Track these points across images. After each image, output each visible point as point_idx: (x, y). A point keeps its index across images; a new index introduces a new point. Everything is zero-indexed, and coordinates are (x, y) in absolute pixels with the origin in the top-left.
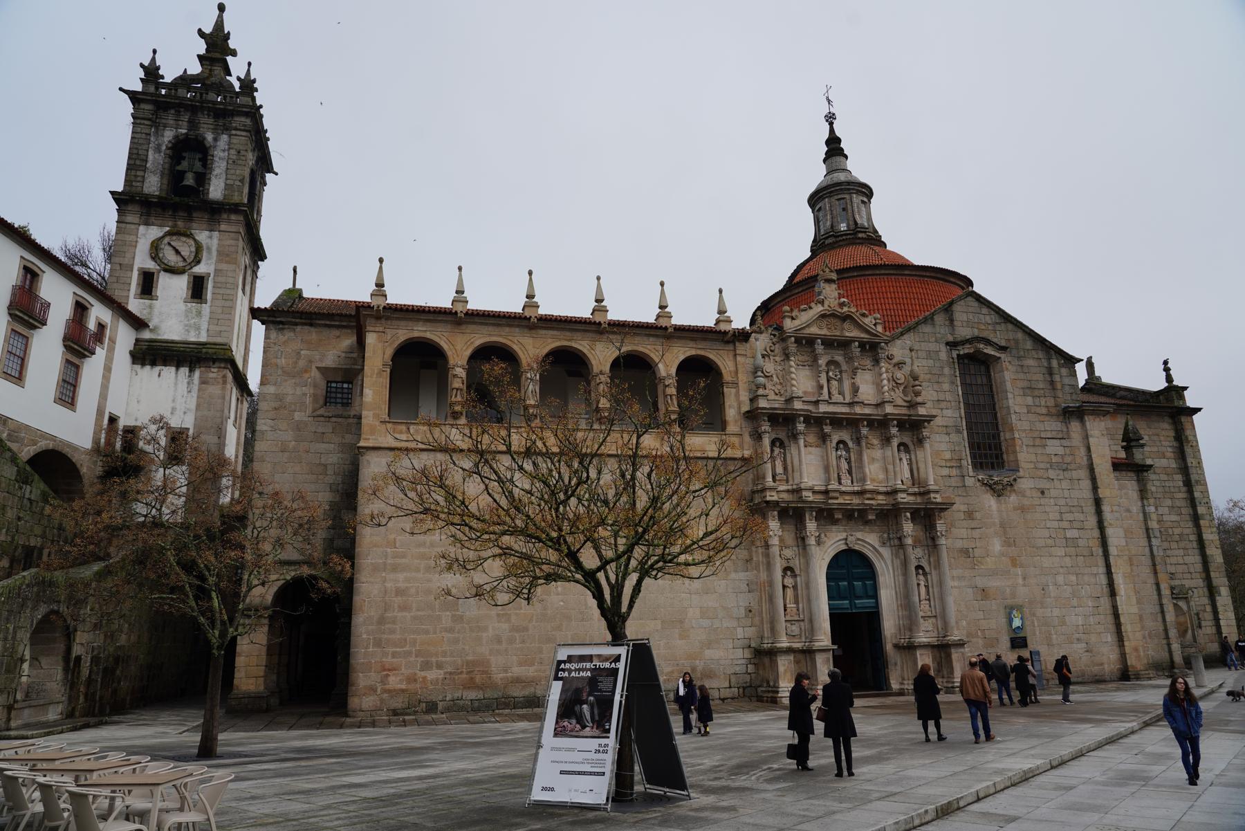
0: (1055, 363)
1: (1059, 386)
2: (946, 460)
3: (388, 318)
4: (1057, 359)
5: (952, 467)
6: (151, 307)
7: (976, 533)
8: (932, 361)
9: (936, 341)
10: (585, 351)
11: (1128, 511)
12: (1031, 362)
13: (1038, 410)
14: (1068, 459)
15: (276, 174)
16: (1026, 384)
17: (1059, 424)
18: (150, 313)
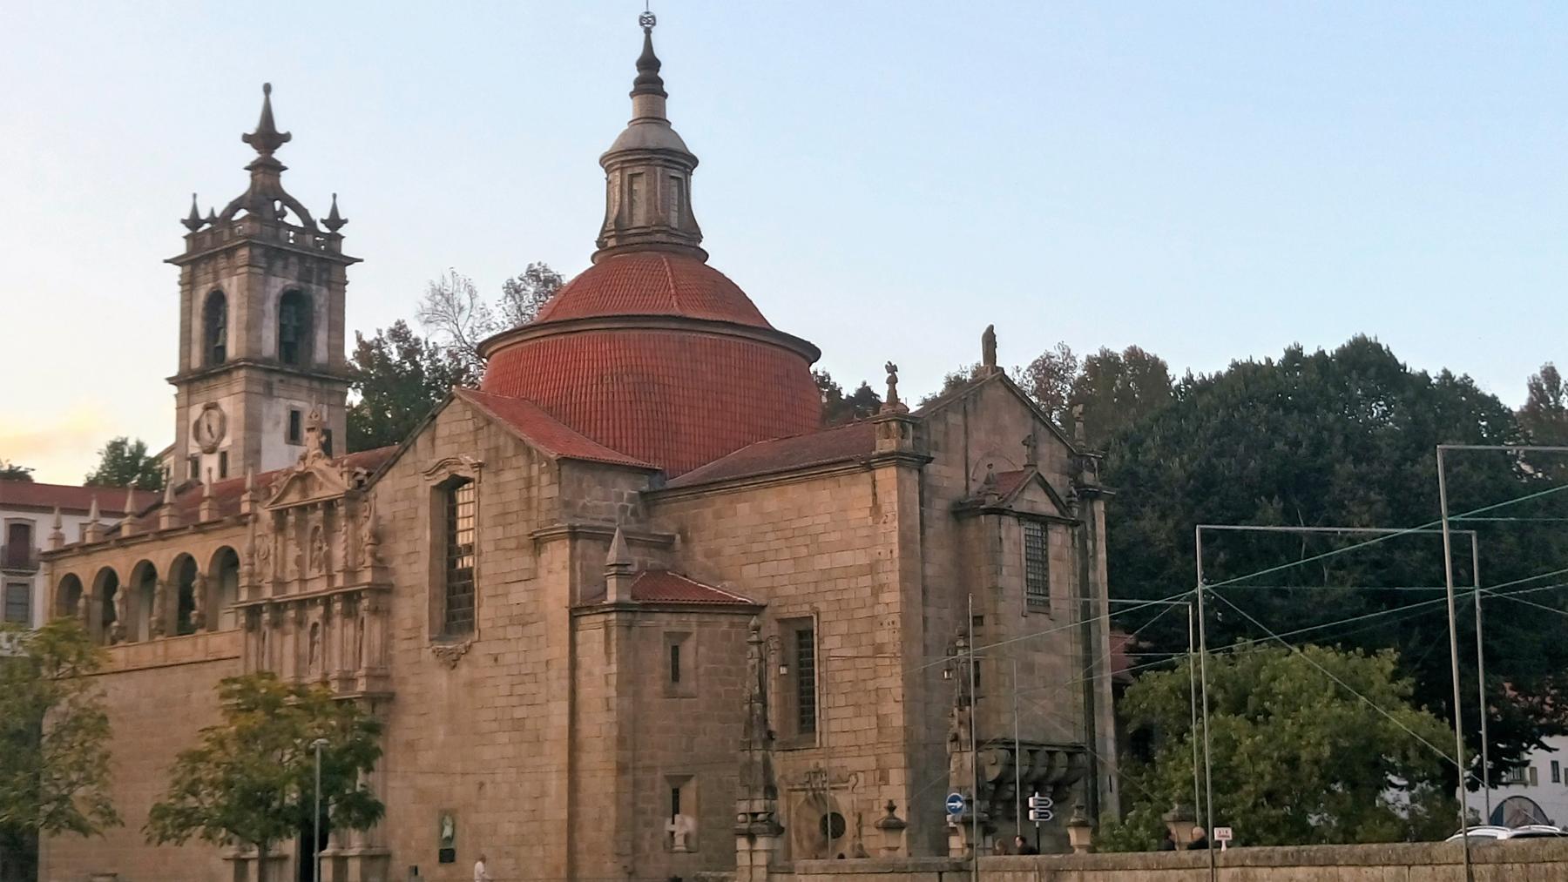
1: (535, 504)
11: (590, 674)
15: (361, 260)
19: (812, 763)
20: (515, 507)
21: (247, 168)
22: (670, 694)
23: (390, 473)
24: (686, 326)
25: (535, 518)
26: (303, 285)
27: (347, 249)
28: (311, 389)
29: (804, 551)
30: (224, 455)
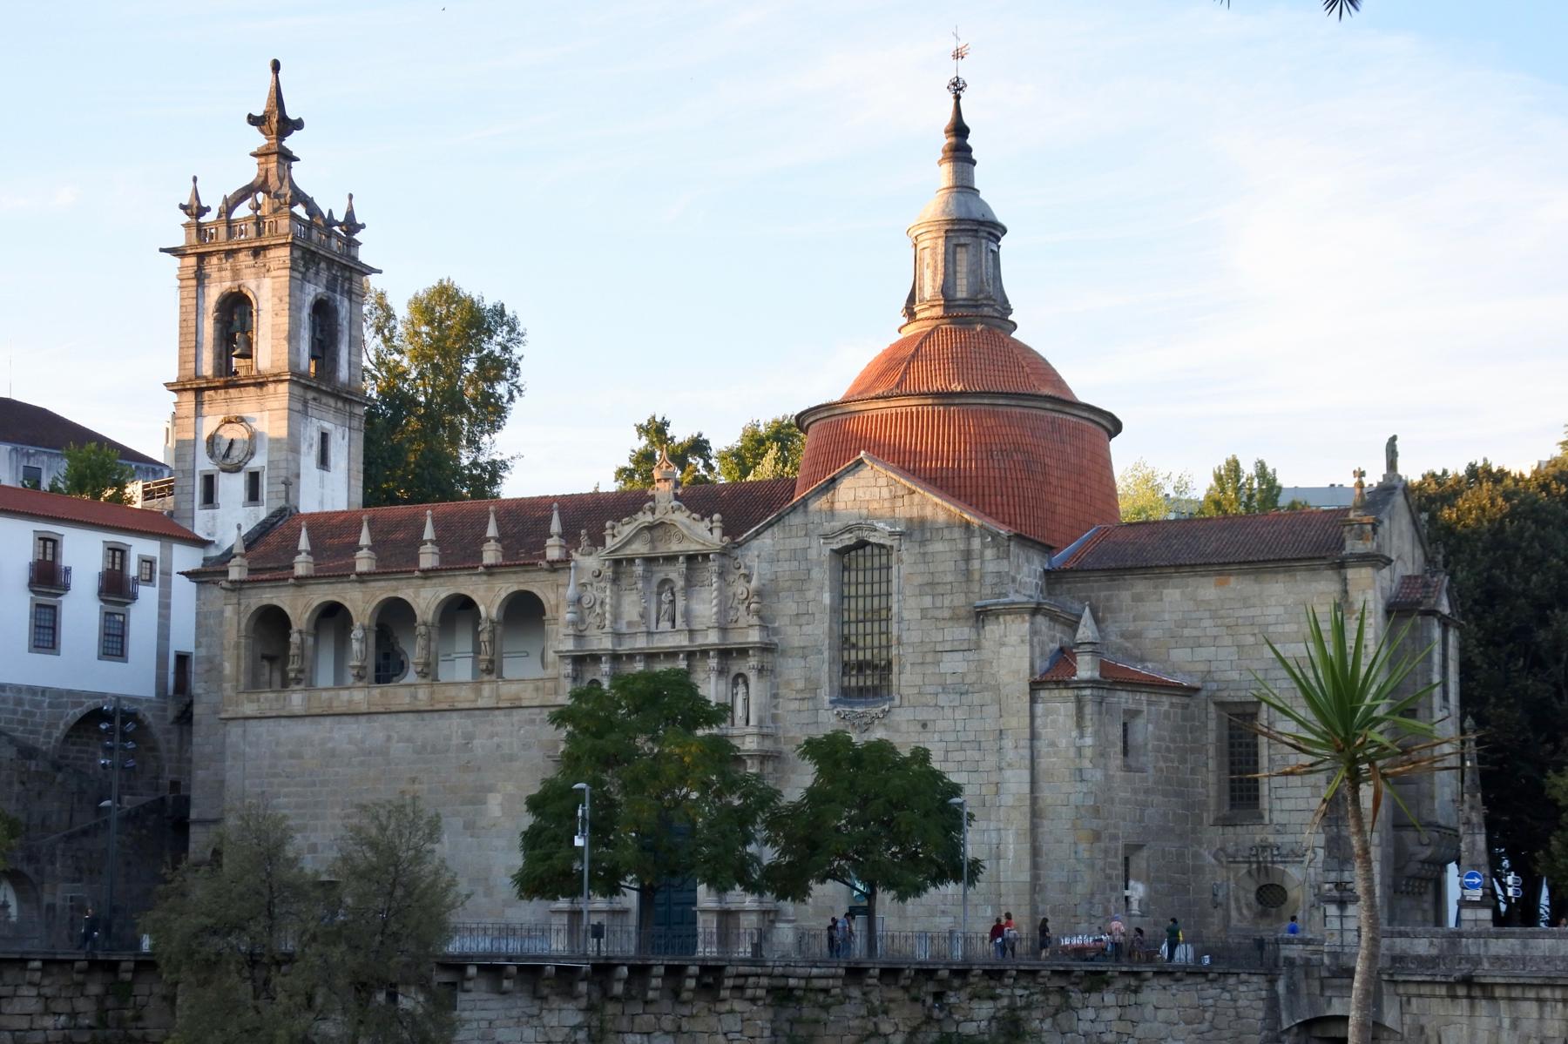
0: (976, 543)
1: (977, 576)
2: (797, 692)
3: (240, 589)
4: (983, 537)
5: (803, 699)
6: (214, 518)
9: (806, 535)
10: (409, 600)
11: (1053, 744)
12: (938, 547)
13: (938, 613)
14: (970, 679)
16: (927, 578)
17: (966, 630)
18: (214, 525)
19: (1258, 839)
20: (949, 578)
21: (254, 155)
22: (1127, 768)
23: (770, 531)
24: (1058, 407)
25: (977, 590)
26: (330, 293)
27: (365, 256)
28: (337, 410)
29: (1251, 640)
30: (254, 478)
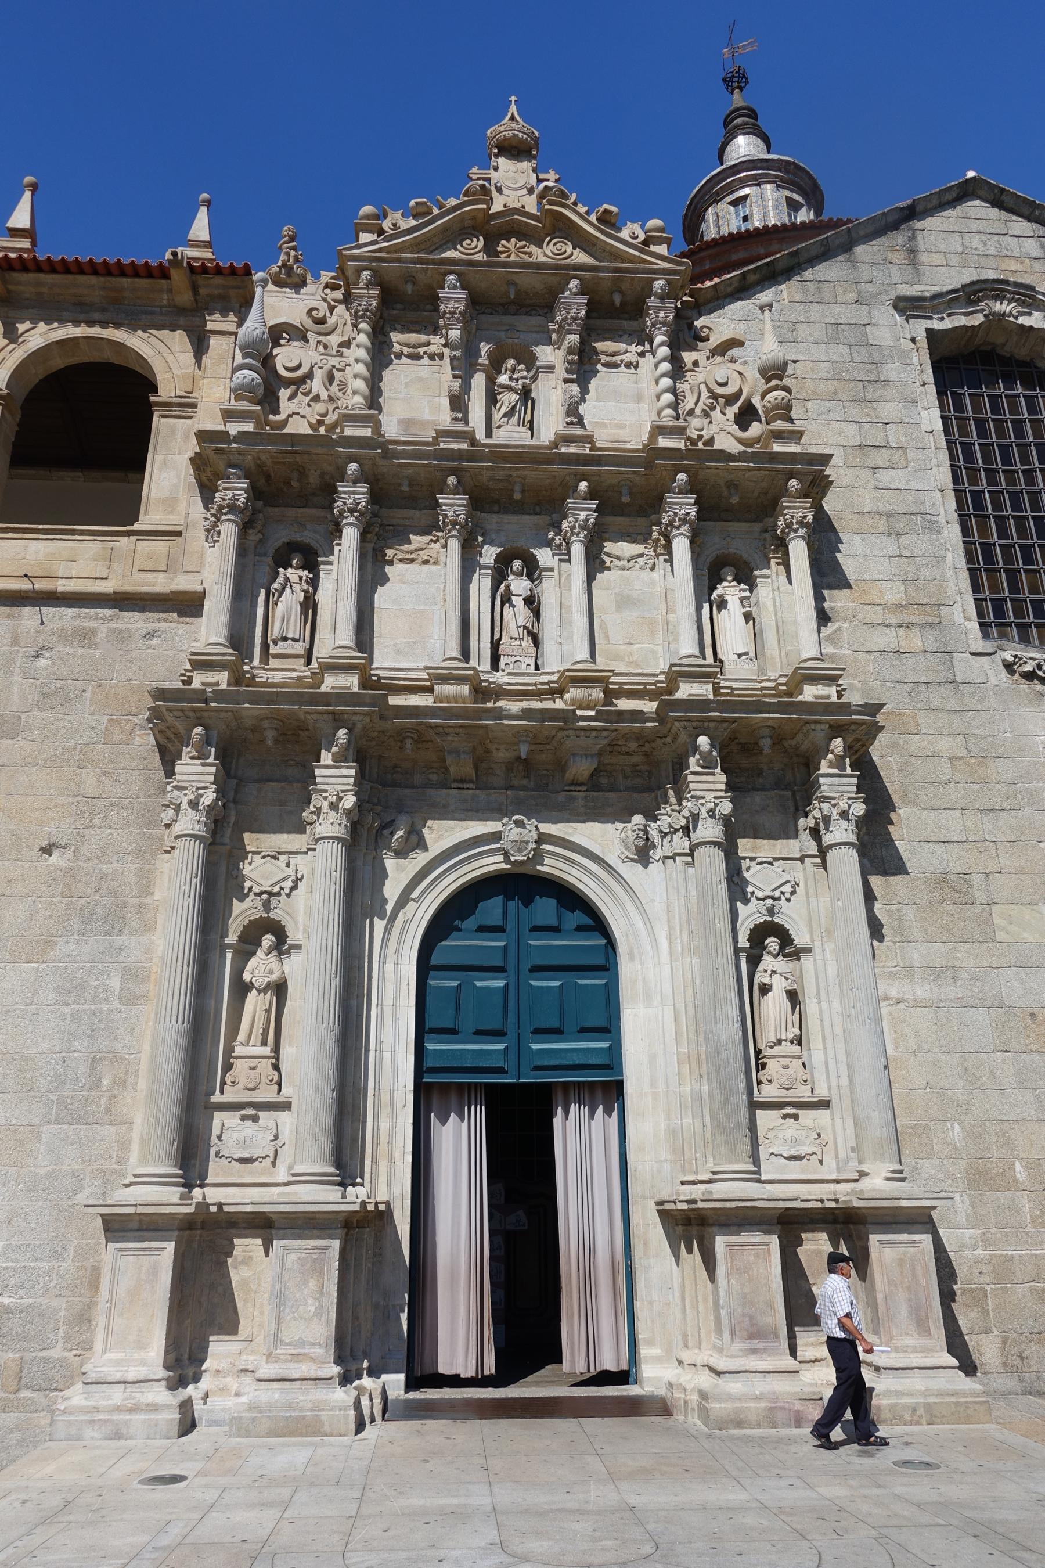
2: (886, 608)
5: (909, 626)
7: (1000, 827)
8: (844, 350)
